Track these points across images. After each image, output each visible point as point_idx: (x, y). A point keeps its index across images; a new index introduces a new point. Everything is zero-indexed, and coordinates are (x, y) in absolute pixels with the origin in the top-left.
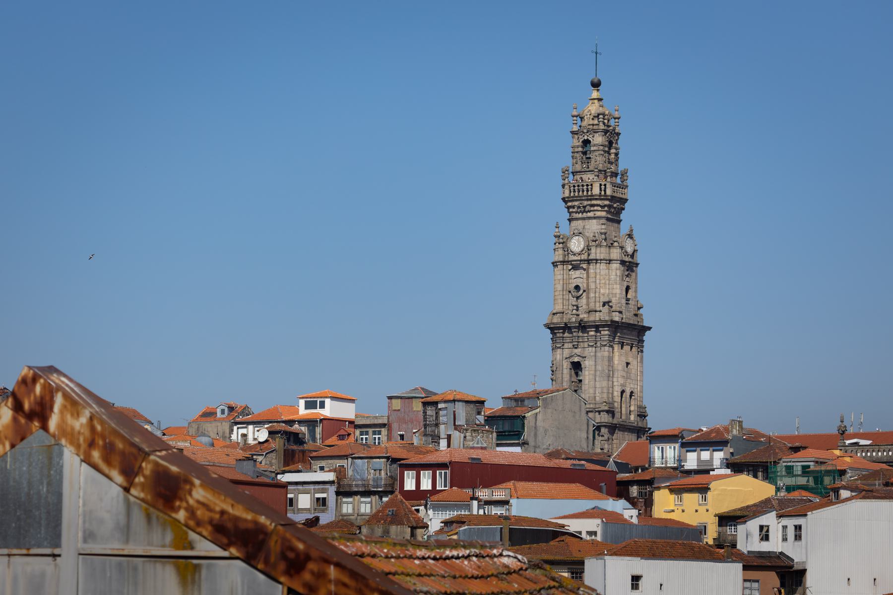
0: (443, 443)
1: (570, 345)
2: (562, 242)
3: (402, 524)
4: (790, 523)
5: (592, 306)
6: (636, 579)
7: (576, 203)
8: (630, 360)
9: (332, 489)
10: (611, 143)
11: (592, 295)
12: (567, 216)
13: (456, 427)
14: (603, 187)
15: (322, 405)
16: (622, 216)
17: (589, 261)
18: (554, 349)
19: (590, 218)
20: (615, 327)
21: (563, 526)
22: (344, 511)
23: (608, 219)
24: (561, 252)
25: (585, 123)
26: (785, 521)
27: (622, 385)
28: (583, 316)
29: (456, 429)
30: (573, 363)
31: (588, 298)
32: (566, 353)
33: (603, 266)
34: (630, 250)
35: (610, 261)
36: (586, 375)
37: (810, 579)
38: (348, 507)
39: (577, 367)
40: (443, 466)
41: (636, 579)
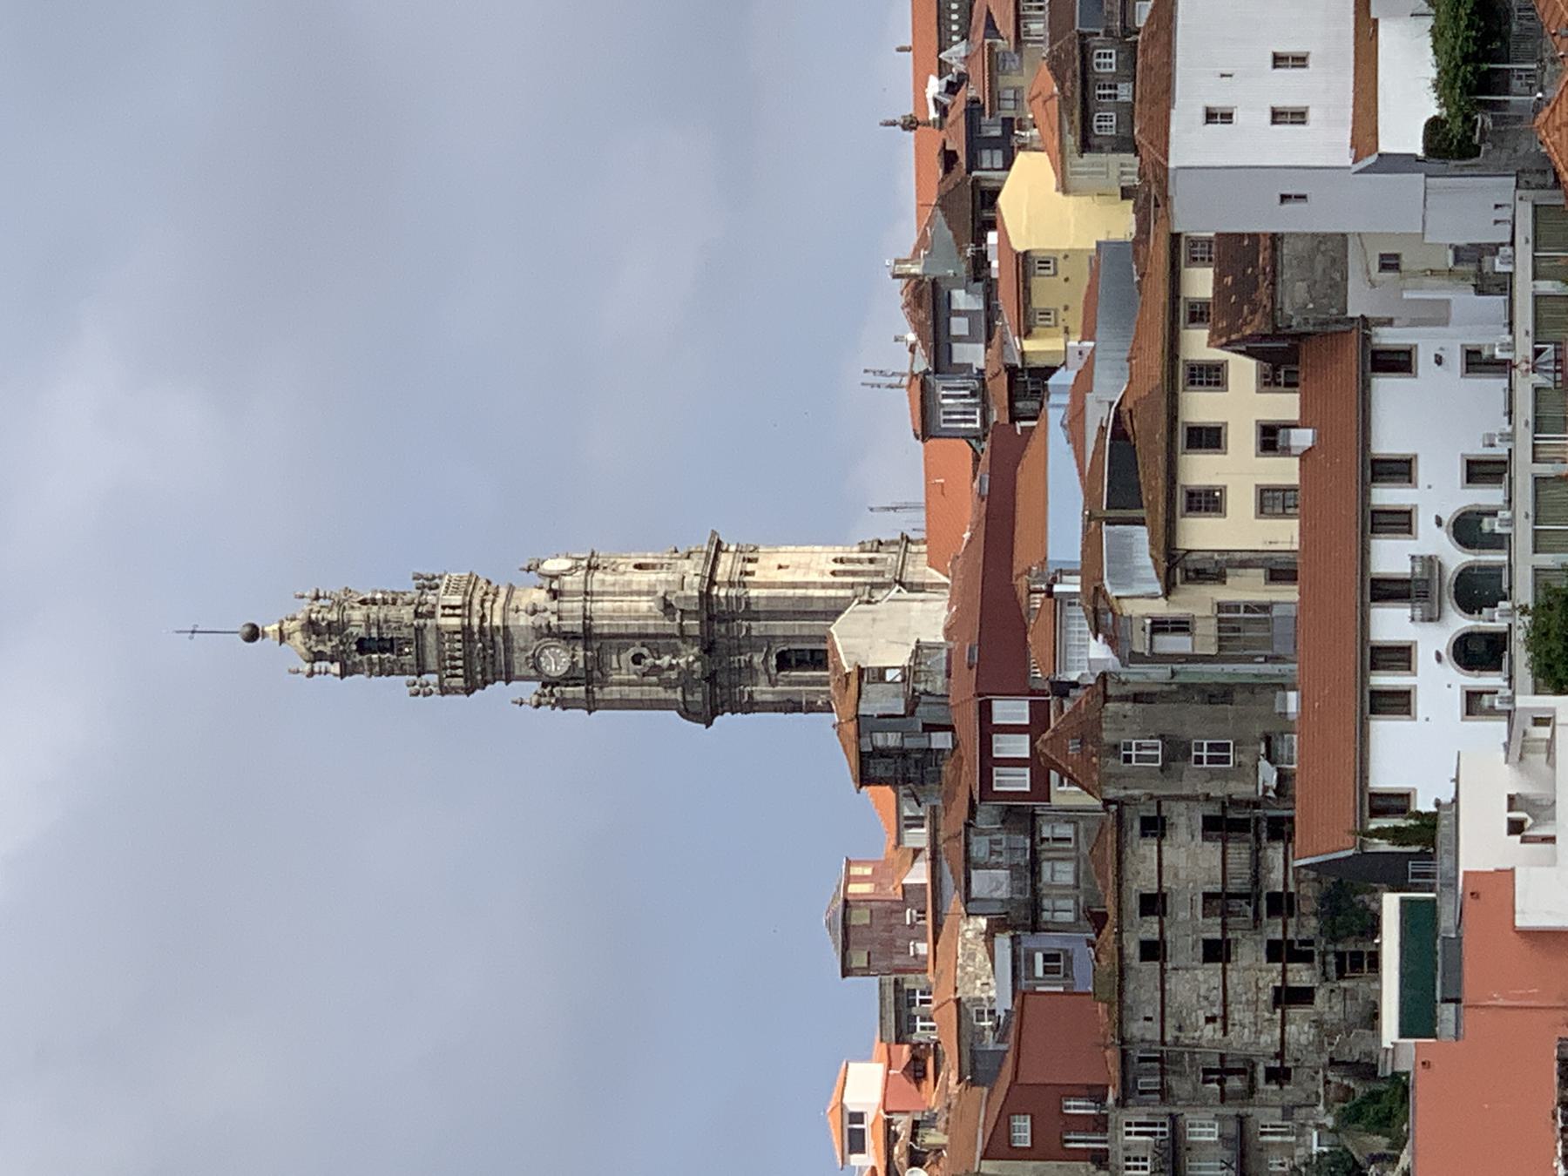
0: (941, 740)
3: (1098, 724)
6: (1210, 116)
8: (774, 563)
9: (1028, 941)
10: (363, 602)
11: (651, 631)
12: (500, 684)
14: (448, 611)
15: (858, 1117)
18: (751, 706)
21: (1102, 429)
22: (1069, 917)
27: (822, 573)
29: (912, 713)
30: (780, 668)
38: (1061, 910)
40: (985, 710)
41: (1210, 116)
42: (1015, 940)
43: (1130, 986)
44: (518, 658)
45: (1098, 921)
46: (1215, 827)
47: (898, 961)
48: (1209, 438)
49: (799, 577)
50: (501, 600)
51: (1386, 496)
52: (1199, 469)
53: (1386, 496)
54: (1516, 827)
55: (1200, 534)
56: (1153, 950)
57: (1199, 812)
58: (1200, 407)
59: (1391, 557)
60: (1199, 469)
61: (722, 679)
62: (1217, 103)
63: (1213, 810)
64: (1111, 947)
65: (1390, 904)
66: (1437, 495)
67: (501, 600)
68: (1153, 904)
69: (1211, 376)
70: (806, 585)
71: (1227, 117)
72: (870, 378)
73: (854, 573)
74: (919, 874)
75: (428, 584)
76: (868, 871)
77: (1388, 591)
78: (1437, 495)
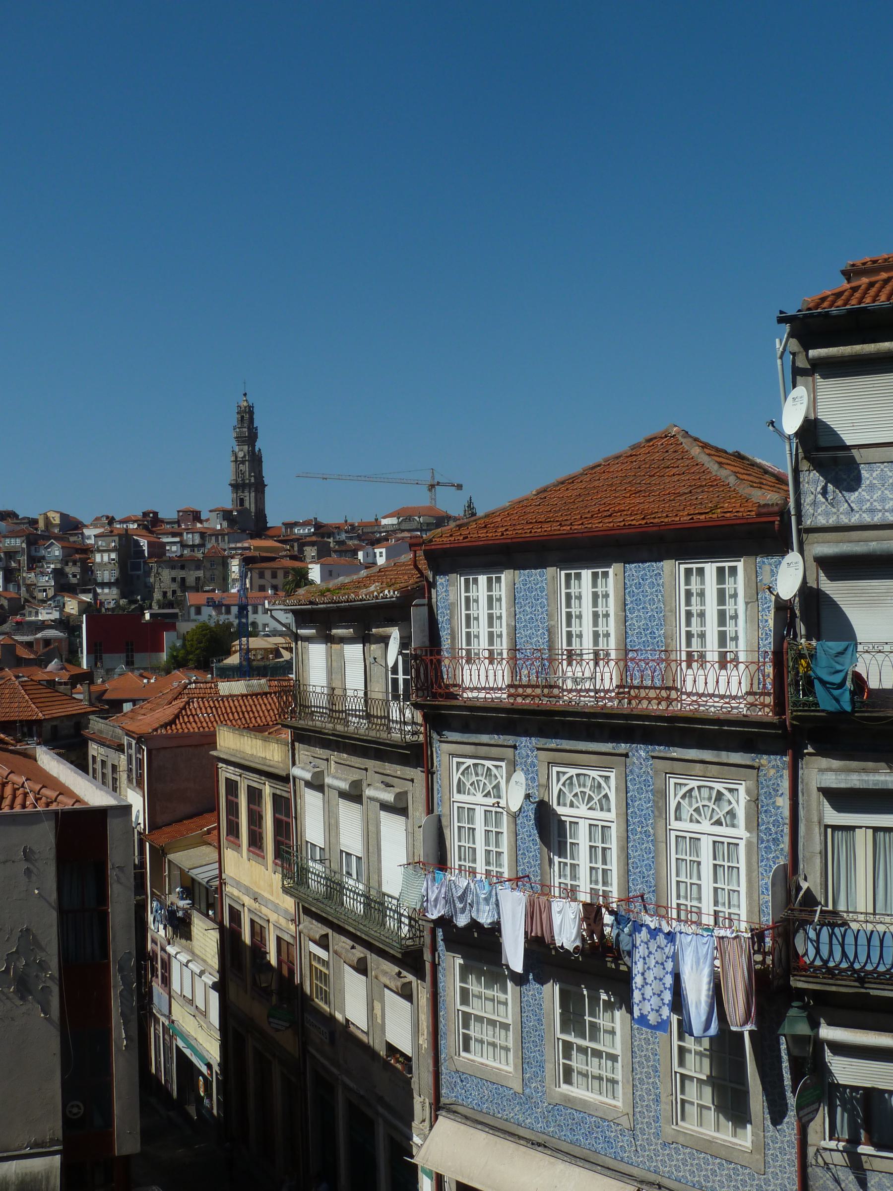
4: (377, 551)
7: (240, 440)
9: (179, 545)
26: (376, 550)
39: (242, 501)
46: (198, 579)
48: (274, 576)
52: (268, 574)
55: (256, 576)
58: (280, 574)
60: (268, 574)
69: (286, 574)
75: (256, 429)
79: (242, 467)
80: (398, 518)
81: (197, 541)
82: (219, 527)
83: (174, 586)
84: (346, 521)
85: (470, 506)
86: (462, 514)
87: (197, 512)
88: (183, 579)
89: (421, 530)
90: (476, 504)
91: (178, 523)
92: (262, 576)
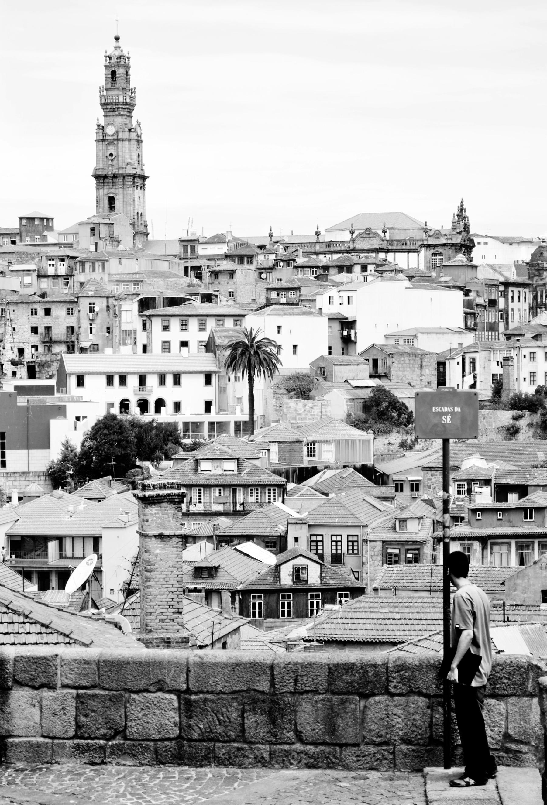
1: (107, 187)
2: (101, 128)
5: (120, 166)
6: (279, 328)
9: (35, 275)
10: (127, 72)
11: (120, 159)
12: (103, 114)
13: (101, 239)
16: (133, 114)
17: (118, 140)
18: (98, 189)
19: (117, 115)
20: (135, 176)
23: (127, 116)
24: (101, 134)
25: (112, 61)
26: (342, 294)
28: (115, 171)
31: (118, 160)
32: (106, 191)
33: (127, 142)
34: (139, 134)
35: (130, 140)
36: (118, 204)
37: (358, 325)
38: (45, 284)
39: (111, 200)
41: (279, 328)
42: (34, 271)
43: (24, 305)
44: (111, 119)
45: (43, 296)
47: (24, 234)
48: (184, 326)
49: (136, 203)
50: (128, 114)
51: (169, 379)
52: (175, 324)
53: (169, 379)
54: (78, 419)
55: (157, 325)
56: (34, 312)
57: (74, 324)
58: (193, 324)
59: (152, 381)
60: (175, 324)
61: (106, 180)
62: (282, 330)
63: (76, 329)
64: (35, 300)
65: (53, 382)
66: (169, 393)
67: (128, 114)
68: (48, 312)
69: (202, 327)
70: (134, 205)
71: (279, 332)
72: (191, 219)
73: (138, 219)
74: (51, 239)
75: (133, 91)
76: (50, 225)
77: (142, 380)
78: (169, 393)
79: (112, 149)
80: (352, 232)
81: (62, 270)
82: (93, 248)
83: (35, 339)
84: (271, 236)
85: (461, 215)
86: (448, 226)
87: (48, 219)
88: (48, 329)
89: (388, 251)
90: (468, 213)
91: (20, 234)
92: (166, 328)
